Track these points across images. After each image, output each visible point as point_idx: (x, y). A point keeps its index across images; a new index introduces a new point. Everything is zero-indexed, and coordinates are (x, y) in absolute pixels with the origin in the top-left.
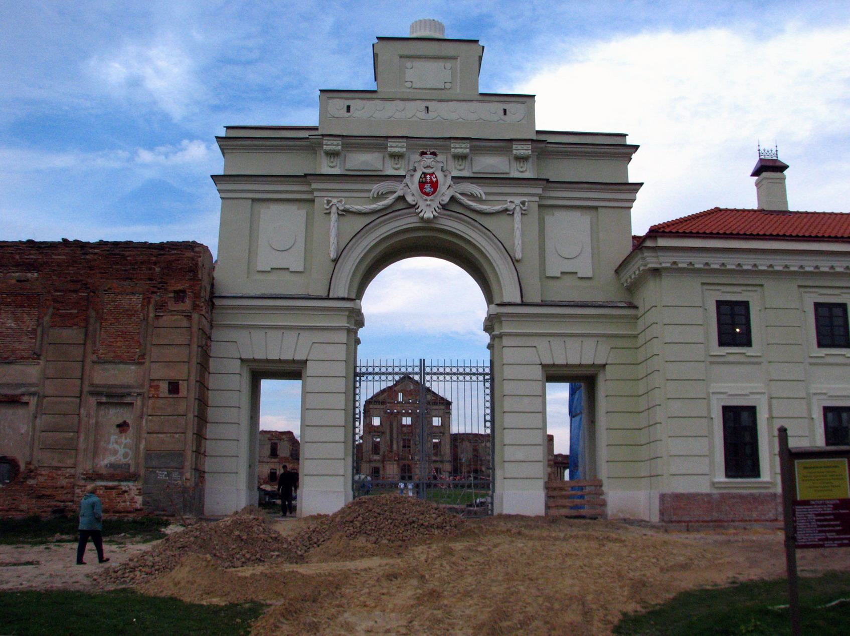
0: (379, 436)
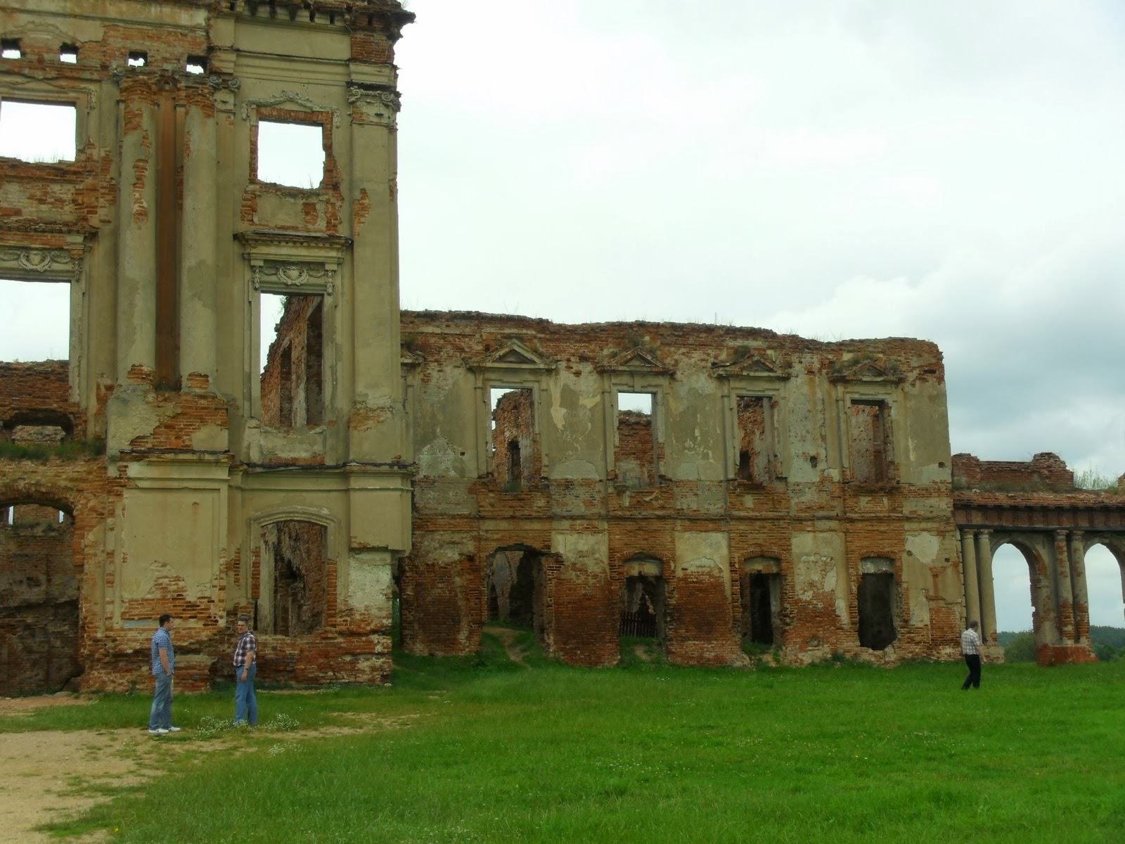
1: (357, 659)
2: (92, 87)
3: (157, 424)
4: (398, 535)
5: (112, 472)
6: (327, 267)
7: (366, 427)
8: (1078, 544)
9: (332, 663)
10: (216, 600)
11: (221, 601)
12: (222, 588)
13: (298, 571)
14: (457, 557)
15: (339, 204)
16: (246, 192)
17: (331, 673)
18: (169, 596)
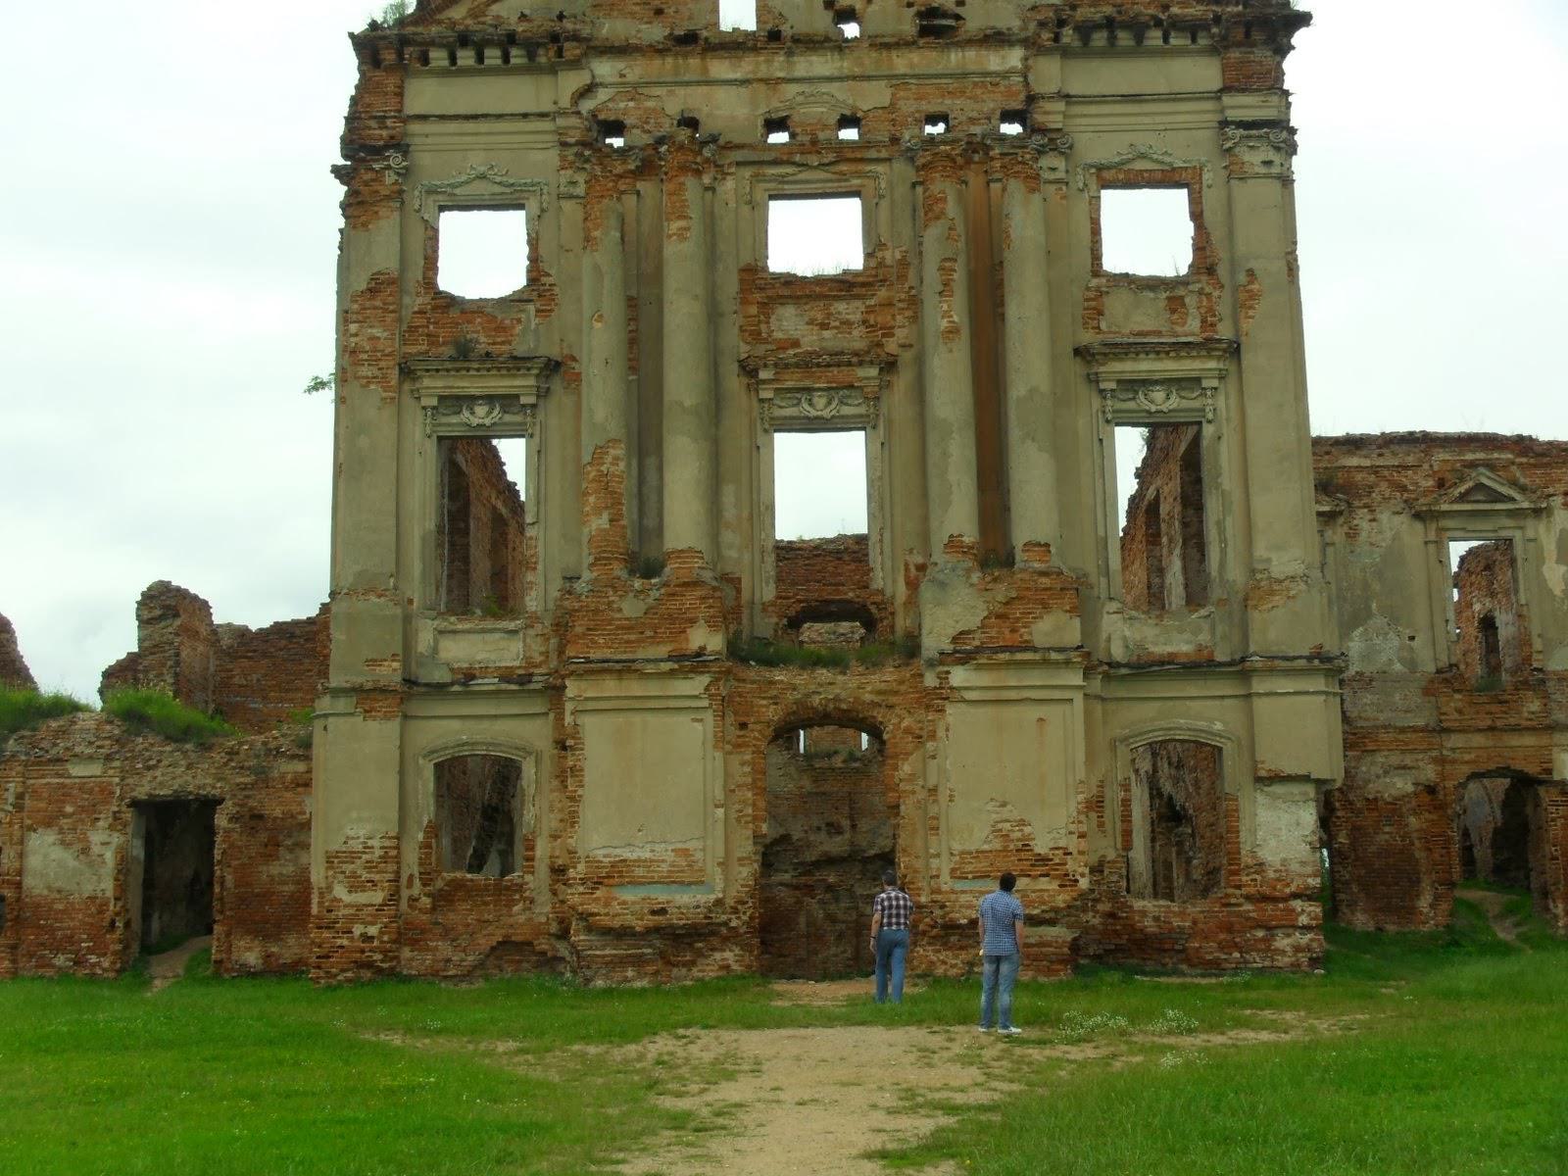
0: (515, 413)
1: (1273, 936)
2: (880, 168)
3: (986, 614)
4: (1325, 760)
5: (930, 680)
6: (1205, 383)
7: (1270, 606)
9: (1237, 940)
10: (1075, 852)
11: (1081, 853)
12: (1082, 836)
13: (1184, 807)
14: (1410, 788)
15: (1216, 293)
16: (1088, 289)
17: (1237, 955)
18: (1012, 847)
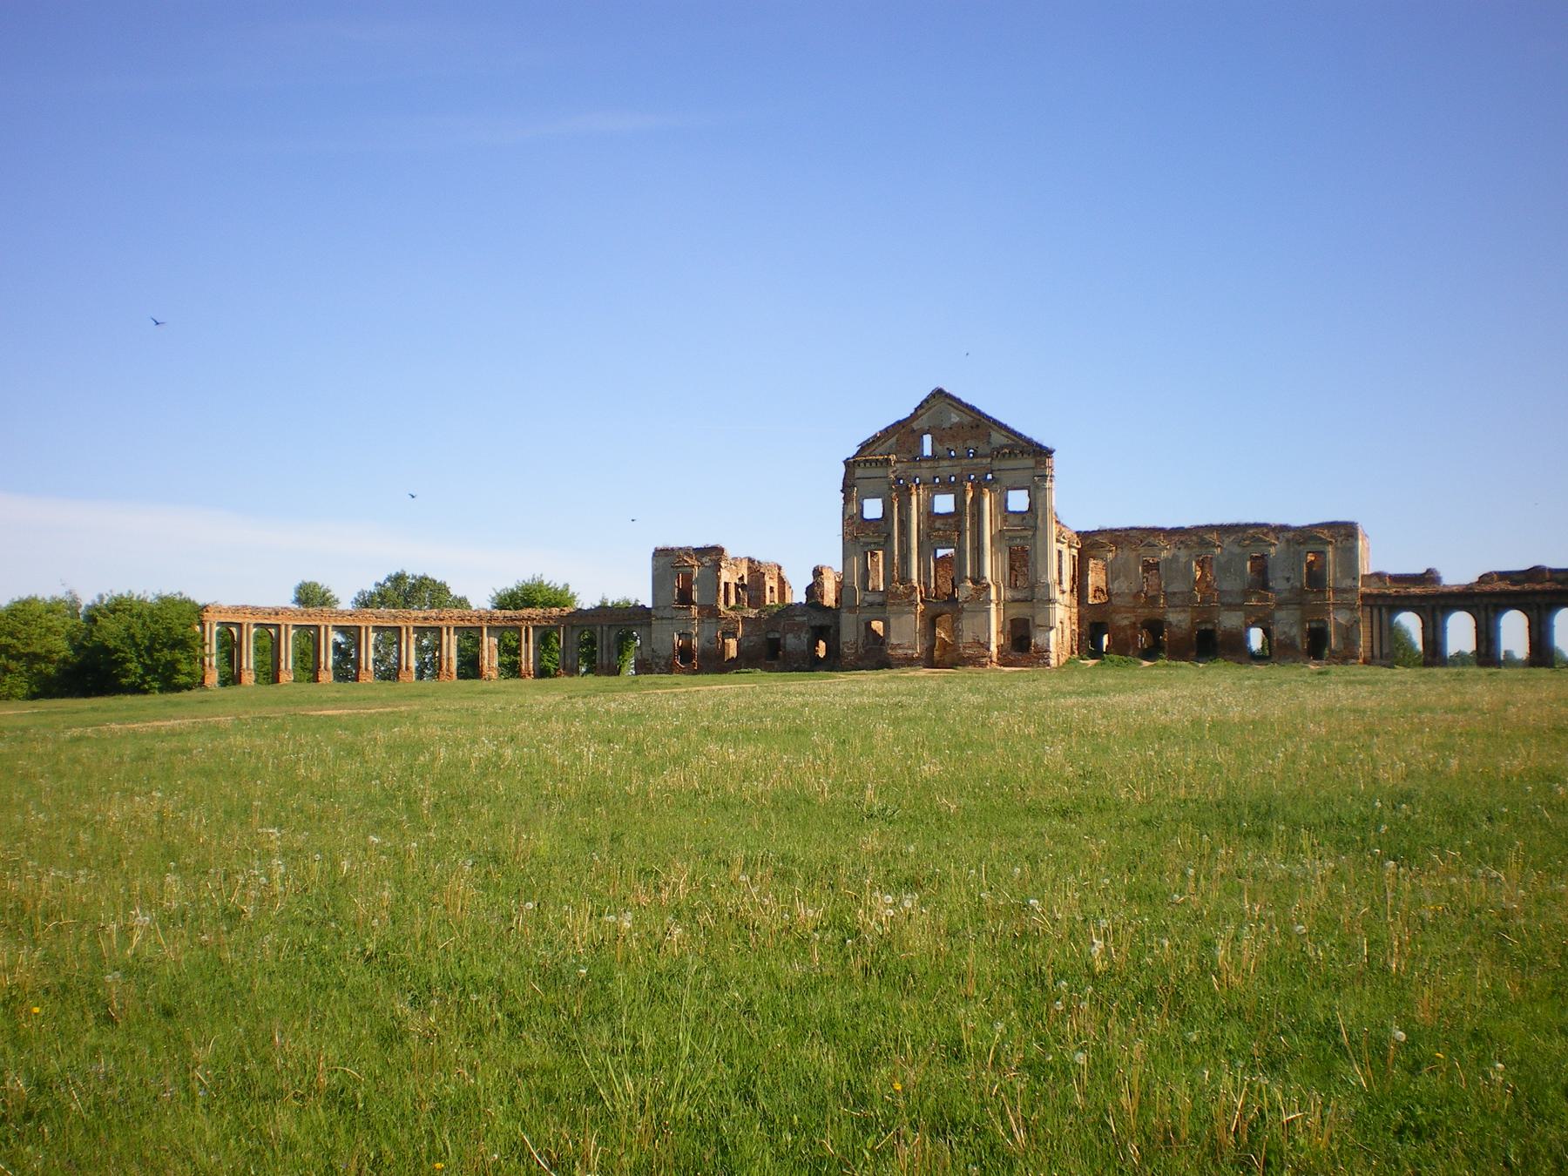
8: (1438, 613)
